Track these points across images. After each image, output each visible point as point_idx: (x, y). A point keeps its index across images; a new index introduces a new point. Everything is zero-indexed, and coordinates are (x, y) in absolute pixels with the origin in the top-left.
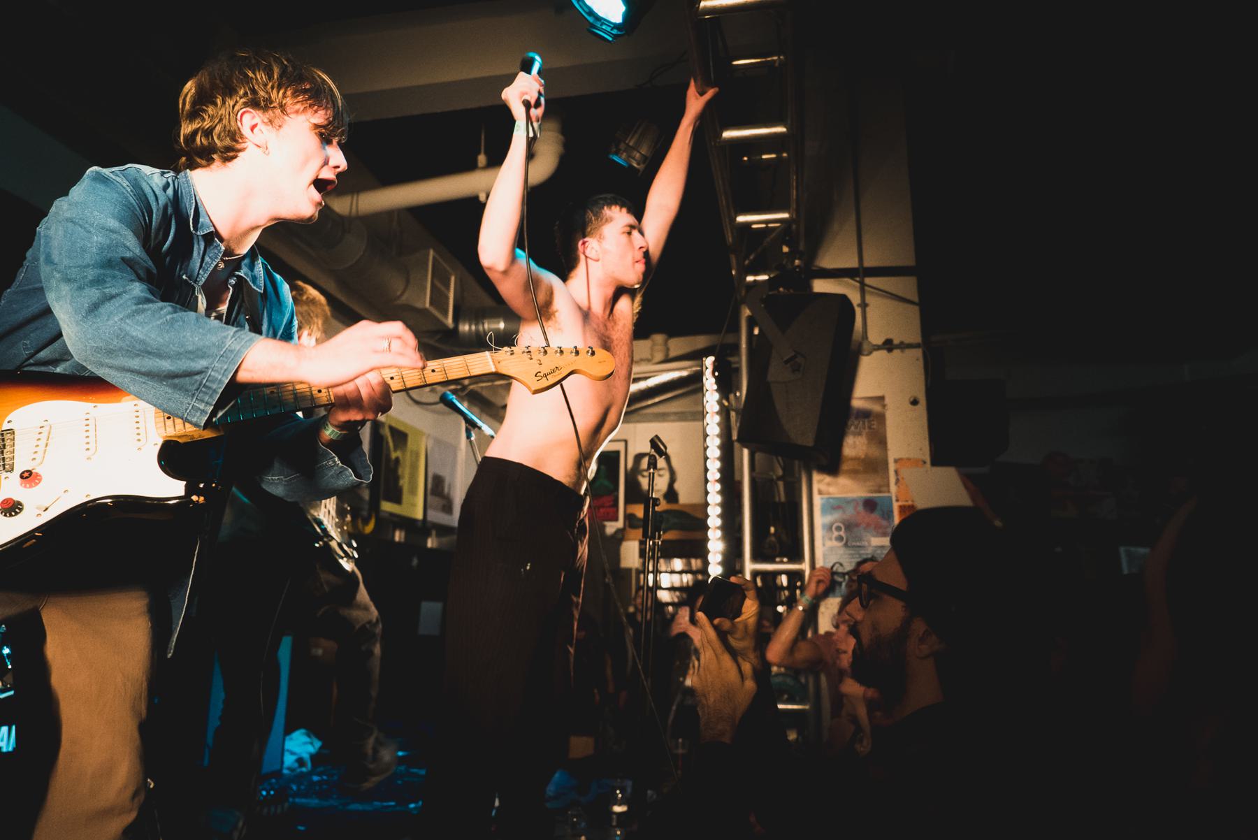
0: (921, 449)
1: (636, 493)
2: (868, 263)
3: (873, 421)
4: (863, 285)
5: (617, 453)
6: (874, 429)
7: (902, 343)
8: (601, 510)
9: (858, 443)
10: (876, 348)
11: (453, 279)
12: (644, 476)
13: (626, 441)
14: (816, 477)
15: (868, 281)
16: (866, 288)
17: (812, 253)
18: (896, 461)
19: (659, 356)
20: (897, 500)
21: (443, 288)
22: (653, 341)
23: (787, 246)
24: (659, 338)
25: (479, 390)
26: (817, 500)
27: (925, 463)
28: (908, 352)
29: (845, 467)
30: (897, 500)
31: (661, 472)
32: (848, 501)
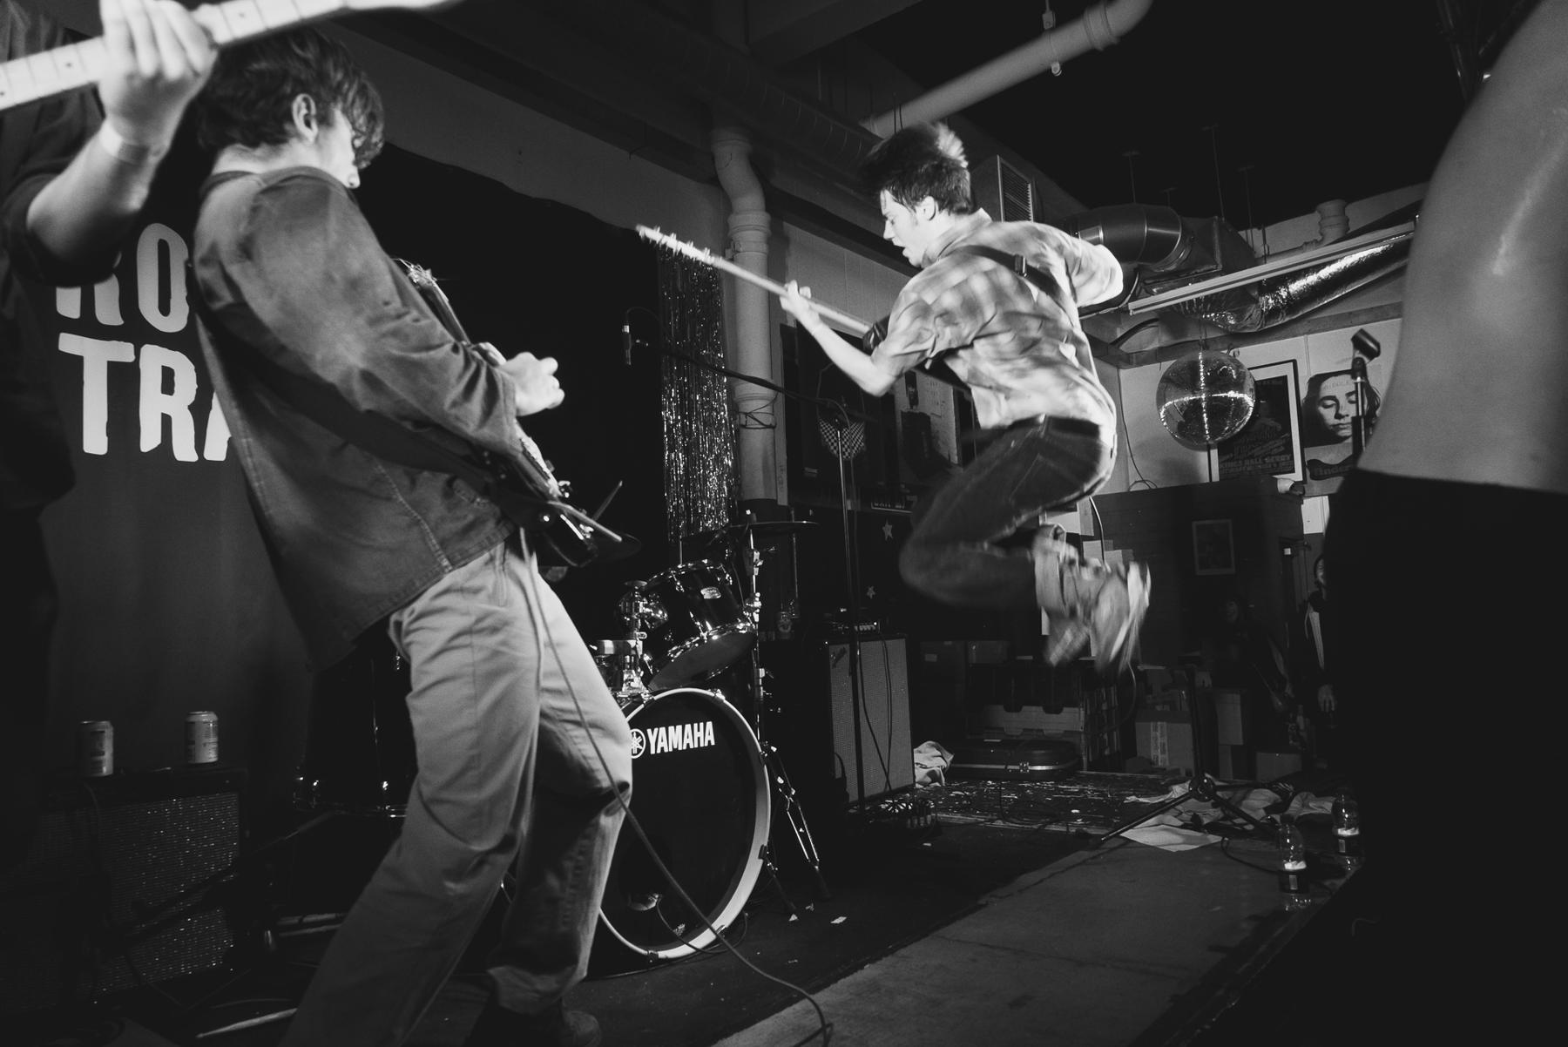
1: (1316, 432)
5: (1284, 378)
11: (1029, 186)
12: (1327, 407)
13: (1294, 362)
19: (1333, 233)
21: (1018, 202)
22: (1320, 212)
24: (1330, 207)
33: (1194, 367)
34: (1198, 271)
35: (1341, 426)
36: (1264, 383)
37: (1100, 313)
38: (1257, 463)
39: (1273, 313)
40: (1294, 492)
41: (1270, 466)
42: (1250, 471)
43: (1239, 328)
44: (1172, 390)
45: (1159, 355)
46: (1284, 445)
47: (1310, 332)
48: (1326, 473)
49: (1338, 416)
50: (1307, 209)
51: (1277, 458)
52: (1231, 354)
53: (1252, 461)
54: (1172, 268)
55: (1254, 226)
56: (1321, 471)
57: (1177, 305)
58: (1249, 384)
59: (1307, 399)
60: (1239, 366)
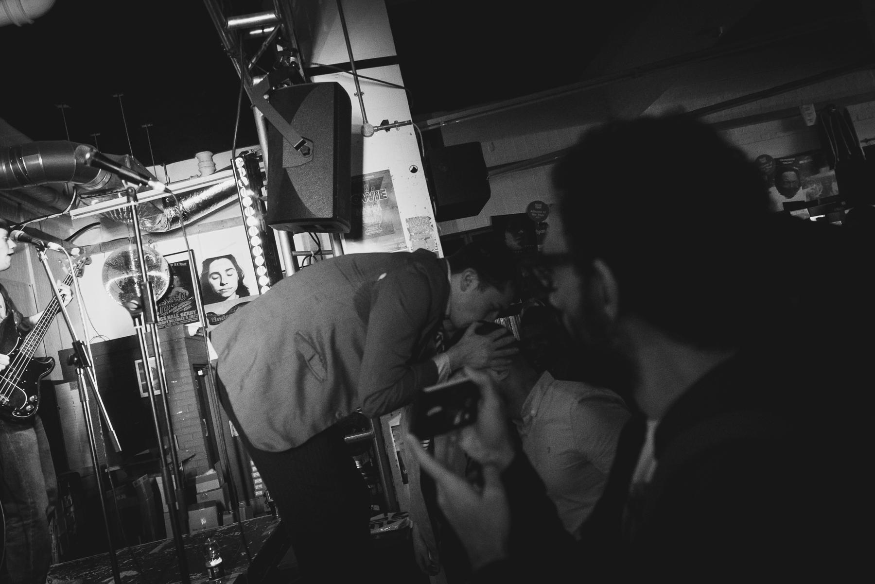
0: (425, 208)
1: (211, 295)
2: (357, 57)
3: (384, 191)
4: (356, 76)
5: (187, 262)
7: (396, 122)
8: (182, 314)
9: (374, 211)
15: (359, 72)
16: (359, 78)
24: (204, 155)
25: (38, 228)
27: (430, 219)
29: (367, 232)
31: (229, 272)
33: (126, 256)
34: (118, 190)
35: (224, 290)
36: (175, 265)
37: (49, 217)
38: (175, 317)
39: (175, 220)
40: (200, 334)
41: (184, 319)
42: (172, 323)
43: (153, 229)
44: (112, 271)
45: (104, 246)
46: (191, 304)
47: (199, 232)
48: (218, 320)
50: (191, 156)
51: (187, 312)
52: (152, 246)
53: (172, 316)
54: (99, 187)
55: (157, 164)
56: (215, 319)
57: (108, 213)
58: (165, 266)
59: (203, 275)
60: (156, 255)
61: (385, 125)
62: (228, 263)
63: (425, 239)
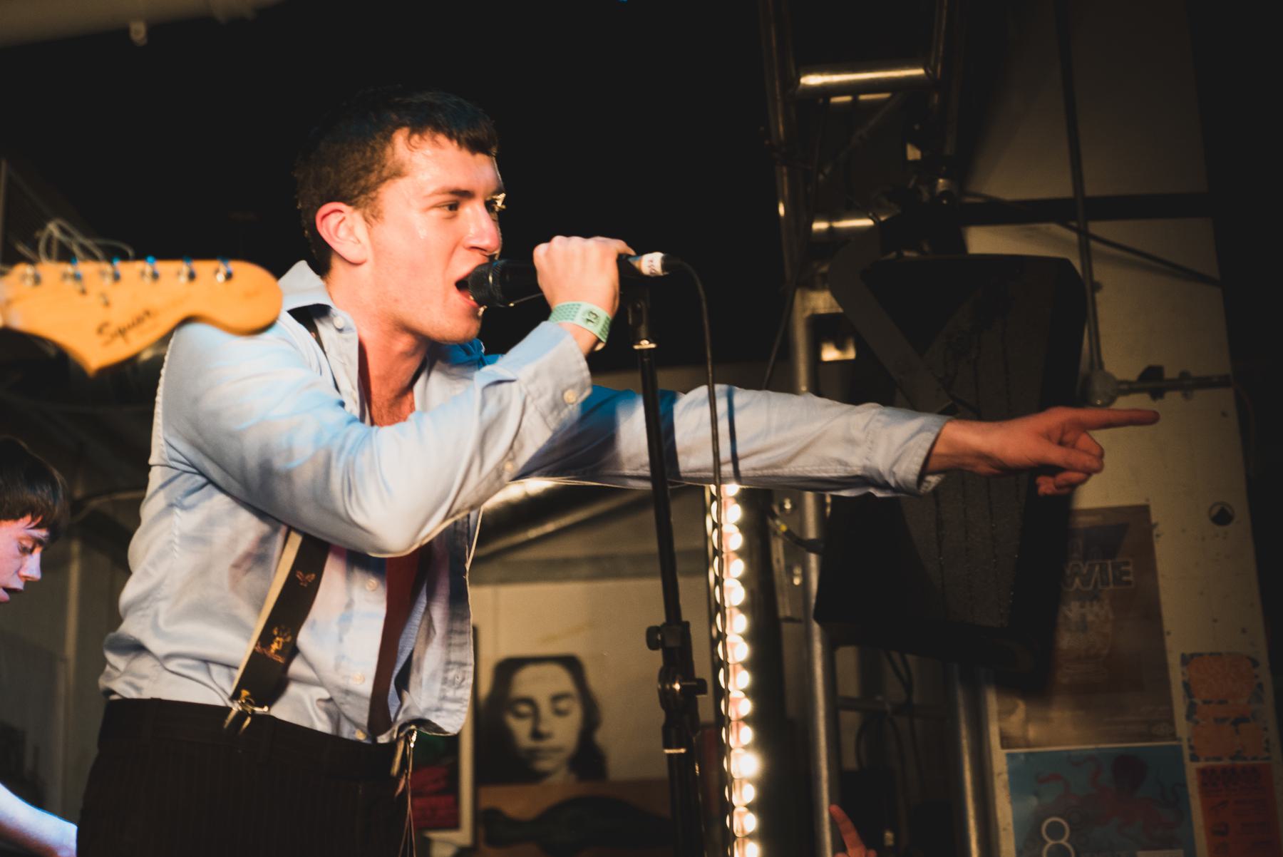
0: (1244, 631)
2: (1092, 189)
3: (1127, 564)
4: (1085, 236)
6: (1129, 583)
7: (1184, 375)
10: (1125, 387)
12: (520, 716)
14: (992, 702)
15: (1096, 228)
16: (1093, 244)
17: (962, 170)
18: (1186, 660)
20: (1194, 758)
23: (918, 145)
26: (999, 760)
27: (1255, 663)
28: (1200, 395)
30: (1194, 758)
31: (563, 705)
32: (1074, 760)
49: (537, 735)
61: (1152, 382)
62: (560, 680)
63: (1236, 722)
